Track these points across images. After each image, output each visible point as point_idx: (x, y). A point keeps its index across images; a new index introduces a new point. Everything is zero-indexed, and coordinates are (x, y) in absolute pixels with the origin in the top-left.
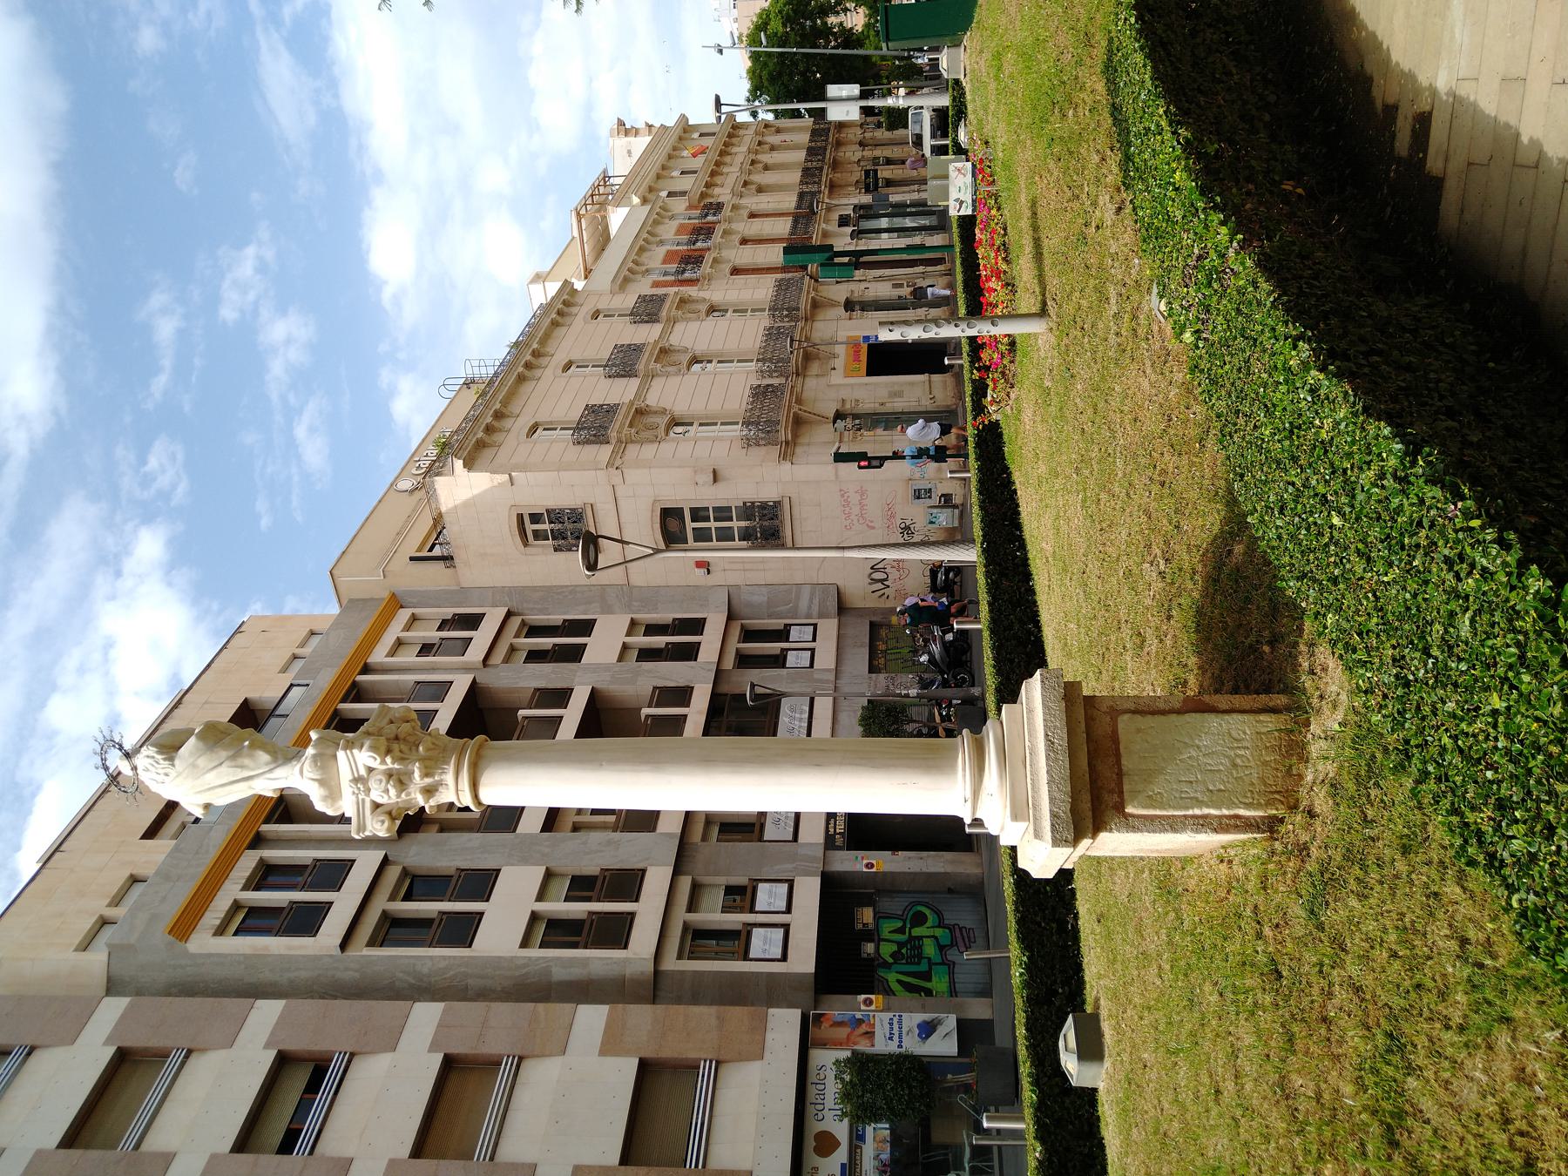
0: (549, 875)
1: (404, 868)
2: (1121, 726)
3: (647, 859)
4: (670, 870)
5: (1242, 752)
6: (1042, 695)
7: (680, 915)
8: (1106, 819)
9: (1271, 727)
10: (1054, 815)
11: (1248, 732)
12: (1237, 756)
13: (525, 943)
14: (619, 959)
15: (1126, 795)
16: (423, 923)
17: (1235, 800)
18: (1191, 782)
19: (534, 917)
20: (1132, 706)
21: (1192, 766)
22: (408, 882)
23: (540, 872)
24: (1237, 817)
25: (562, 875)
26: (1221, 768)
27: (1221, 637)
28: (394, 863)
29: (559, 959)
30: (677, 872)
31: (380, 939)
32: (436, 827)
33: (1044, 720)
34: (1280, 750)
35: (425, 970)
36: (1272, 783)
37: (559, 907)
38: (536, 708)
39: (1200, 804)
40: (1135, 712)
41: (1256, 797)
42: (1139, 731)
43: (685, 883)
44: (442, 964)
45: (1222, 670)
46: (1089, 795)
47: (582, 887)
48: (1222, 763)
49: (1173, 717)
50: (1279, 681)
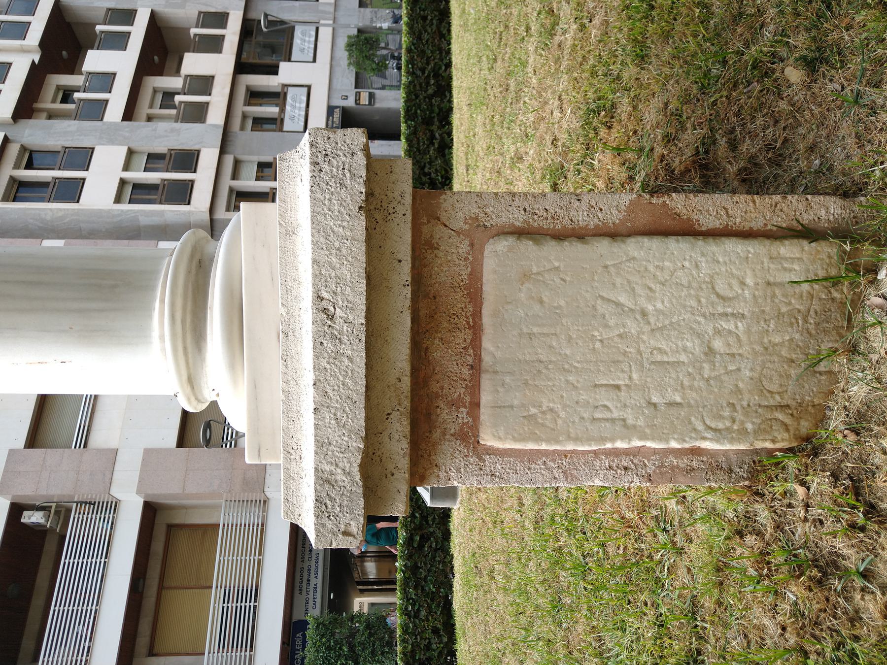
0: (131, 153)
1: (22, 146)
2: (489, 265)
3: (201, 143)
4: (217, 151)
5: (728, 325)
6: (313, 199)
7: (227, 182)
8: (440, 460)
9: (797, 271)
10: (323, 480)
11: (749, 281)
12: (718, 332)
13: (118, 200)
14: (185, 211)
15: (485, 413)
16: (41, 185)
17: (700, 427)
18: (618, 387)
19: (123, 182)
20: (518, 218)
21: (625, 353)
22: (27, 155)
23: (123, 151)
24: (696, 452)
25: (144, 153)
26: (683, 358)
27: (695, 36)
28: (14, 141)
29: (142, 211)
30: (223, 151)
31: (12, 196)
32: (45, 115)
33: (315, 262)
34: (806, 321)
35: (48, 218)
36: (775, 388)
37: (139, 175)
38: (110, 24)
39: (629, 430)
40: (521, 233)
41: (739, 416)
42: (526, 276)
43: (229, 160)
44: (60, 214)
45: (686, 100)
46: (406, 422)
47: (154, 160)
48: (685, 350)
49: (603, 246)
50: (811, 149)
